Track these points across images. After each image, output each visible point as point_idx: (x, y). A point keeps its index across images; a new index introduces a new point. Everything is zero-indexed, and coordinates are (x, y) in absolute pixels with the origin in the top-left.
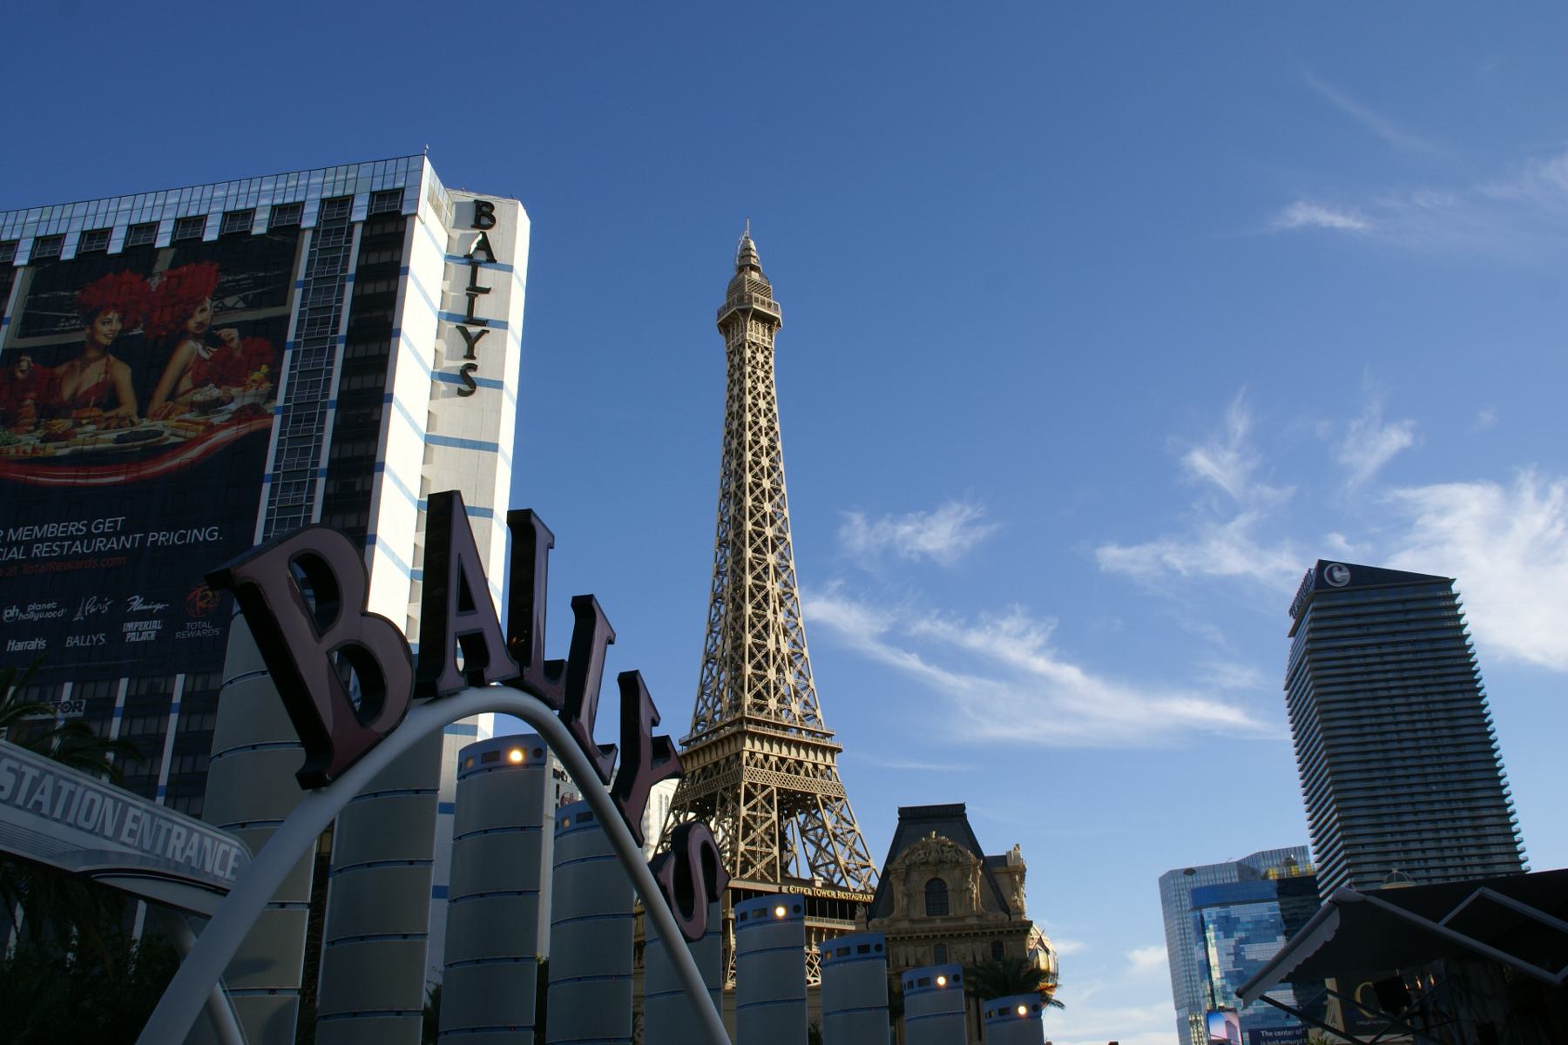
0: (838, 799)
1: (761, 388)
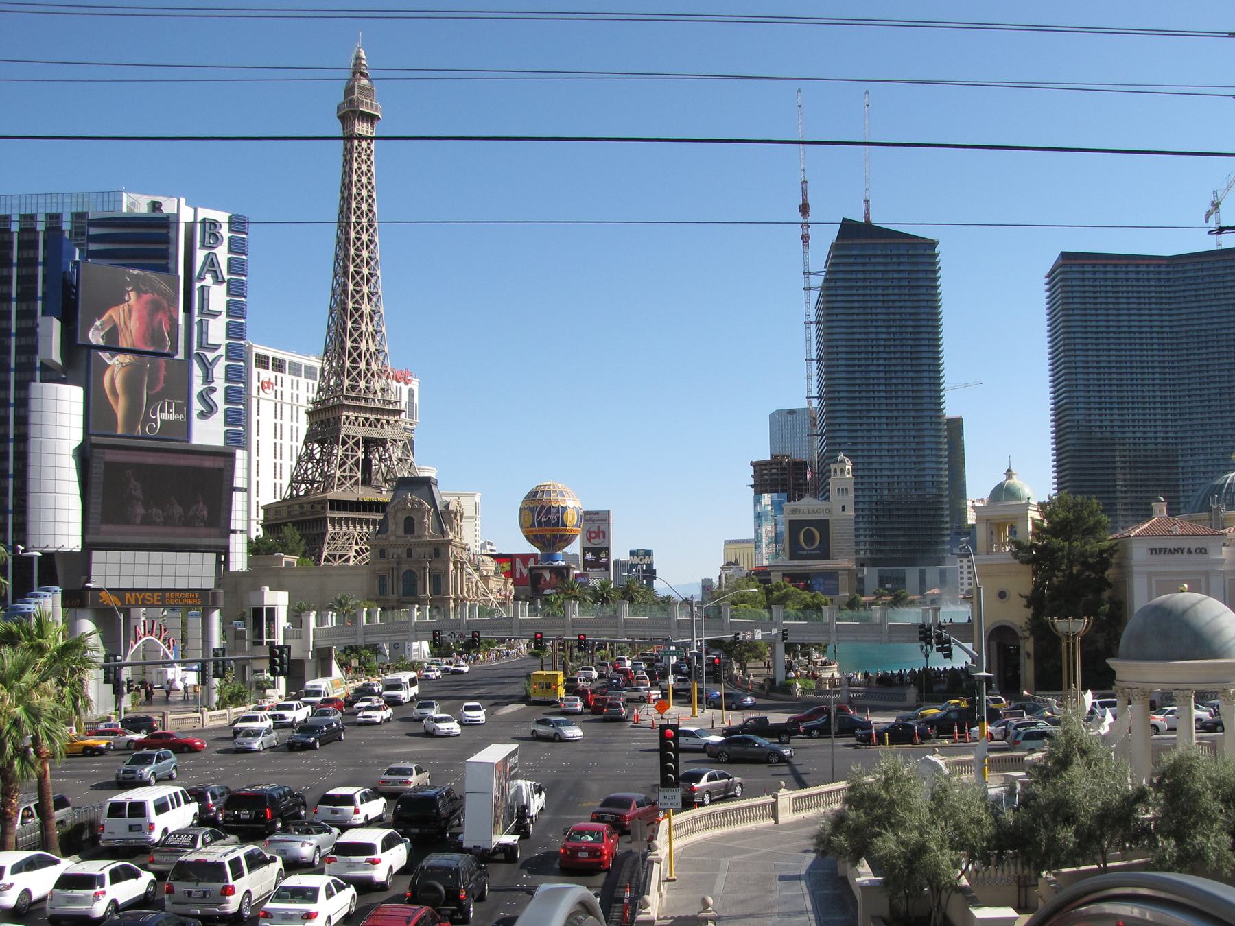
1: (364, 167)
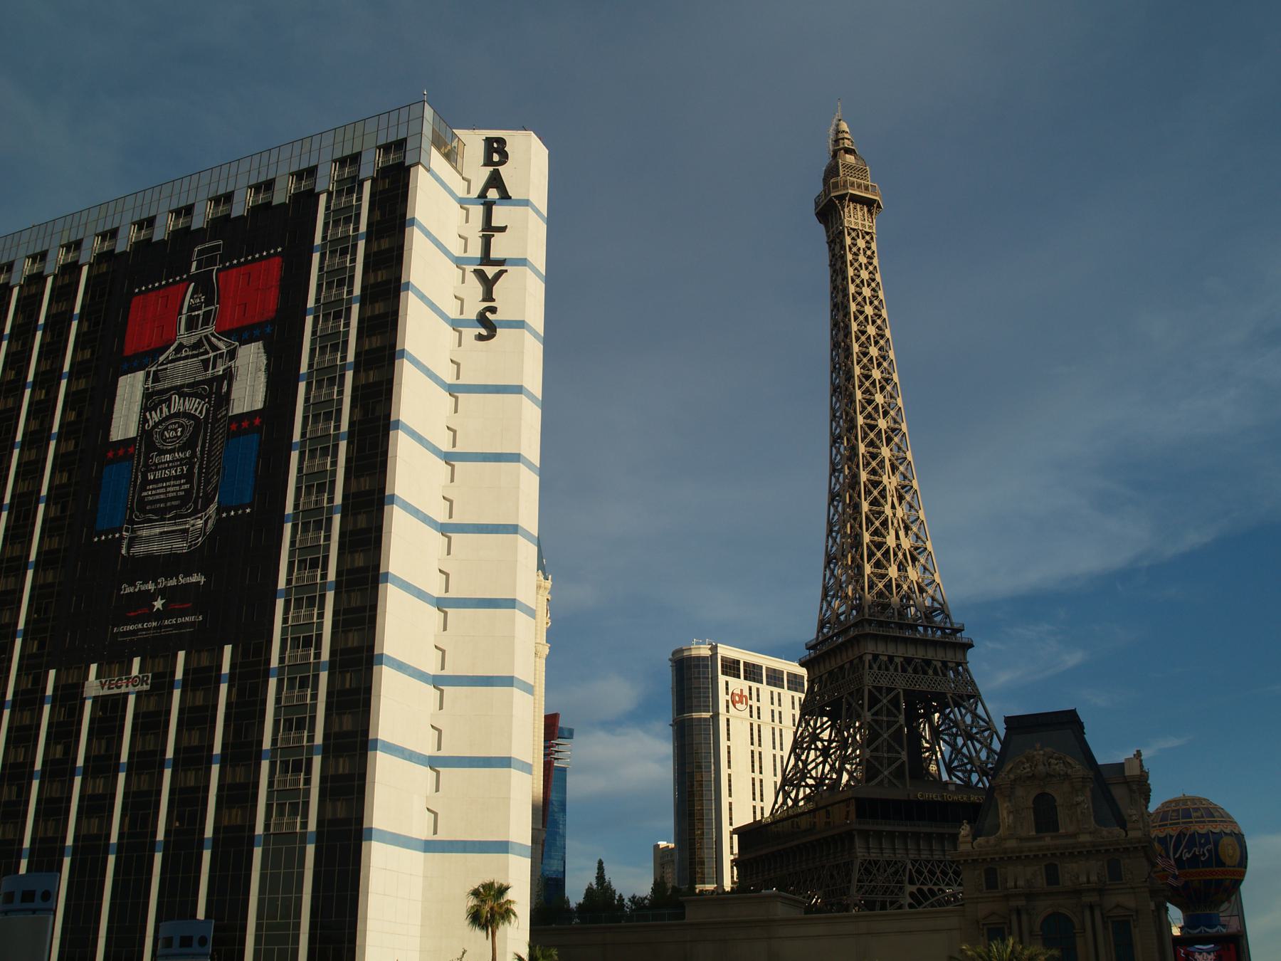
0: (970, 697)
1: (865, 275)
